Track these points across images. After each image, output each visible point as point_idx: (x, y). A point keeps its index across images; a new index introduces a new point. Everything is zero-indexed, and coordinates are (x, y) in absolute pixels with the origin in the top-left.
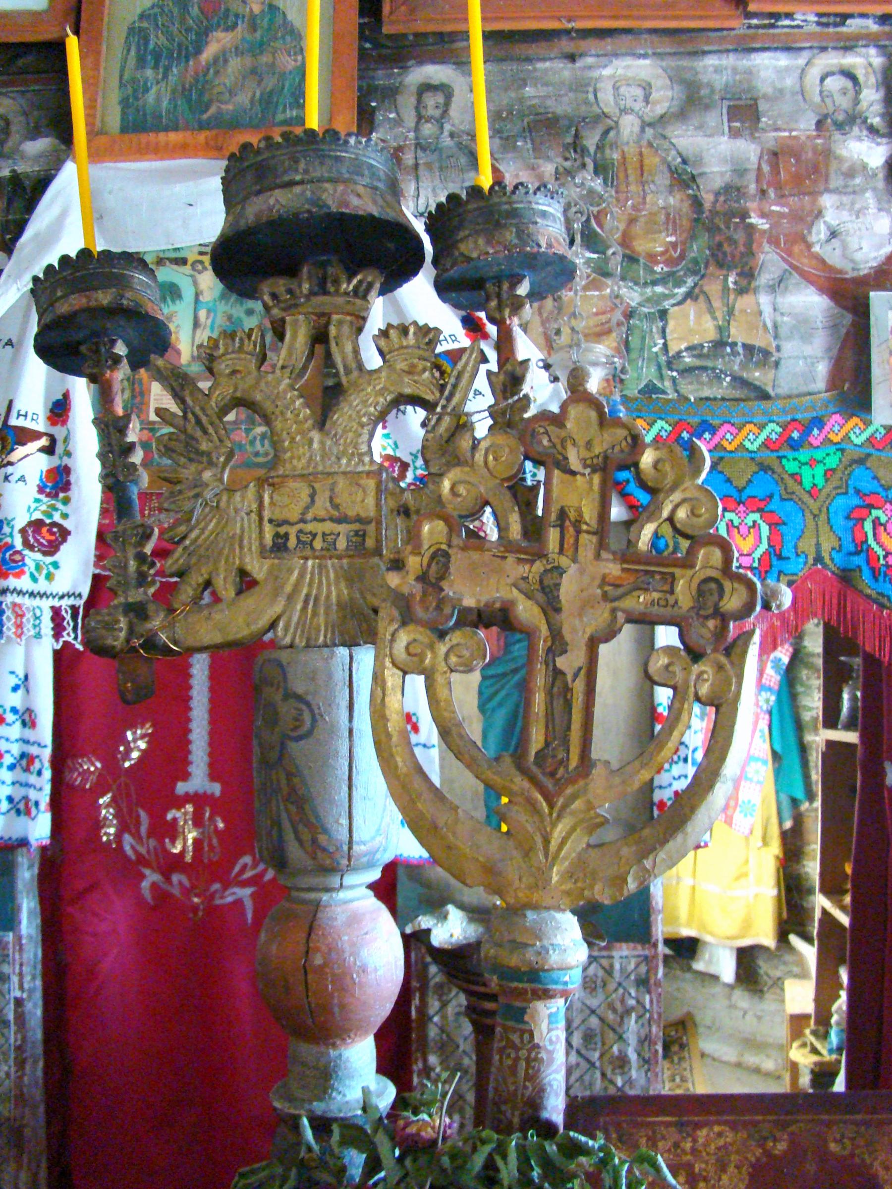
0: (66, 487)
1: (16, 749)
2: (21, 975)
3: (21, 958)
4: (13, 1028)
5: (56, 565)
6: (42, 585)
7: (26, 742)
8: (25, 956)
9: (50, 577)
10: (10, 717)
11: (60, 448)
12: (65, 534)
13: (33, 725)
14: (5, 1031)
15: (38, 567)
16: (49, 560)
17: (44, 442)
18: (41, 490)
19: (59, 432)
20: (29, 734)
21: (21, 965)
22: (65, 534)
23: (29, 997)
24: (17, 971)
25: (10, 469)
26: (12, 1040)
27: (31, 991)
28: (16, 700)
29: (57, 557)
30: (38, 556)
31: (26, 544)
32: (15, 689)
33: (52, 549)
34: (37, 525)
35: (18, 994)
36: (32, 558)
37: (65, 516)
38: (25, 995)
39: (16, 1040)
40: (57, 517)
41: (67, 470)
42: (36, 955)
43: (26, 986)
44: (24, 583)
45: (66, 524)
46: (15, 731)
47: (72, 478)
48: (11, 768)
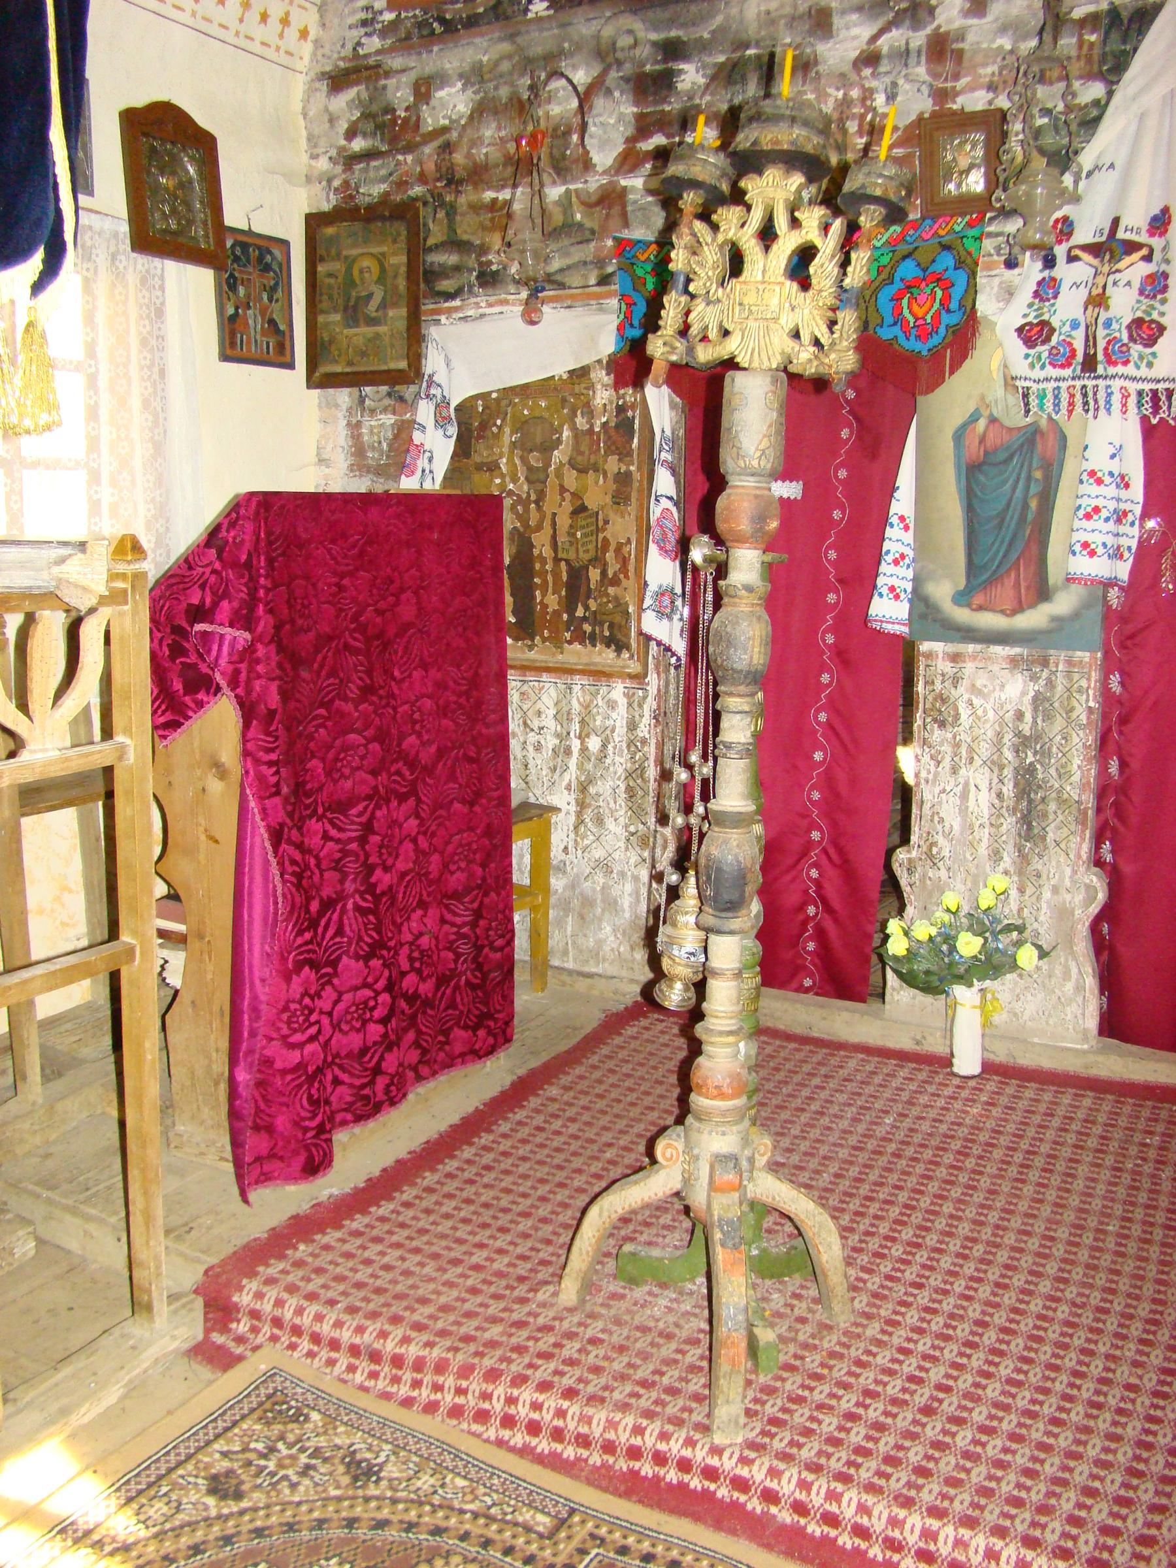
0: (1165, 289)
1: (1112, 505)
5: (1154, 355)
6: (1144, 372)
7: (1118, 500)
9: (1150, 365)
10: (1107, 479)
11: (1157, 256)
12: (1162, 329)
13: (1127, 486)
15: (1141, 358)
16: (1149, 350)
17: (1144, 252)
18: (1141, 293)
19: (1156, 242)
20: (1124, 494)
22: (1162, 329)
25: (1117, 276)
28: (1115, 466)
29: (1155, 349)
30: (1140, 348)
31: (1131, 338)
32: (1113, 457)
33: (1151, 341)
34: (1138, 323)
36: (1136, 349)
37: (1162, 314)
40: (1155, 316)
41: (1165, 276)
44: (1130, 370)
45: (1163, 321)
46: (1111, 491)
47: (1170, 282)
48: (1107, 520)
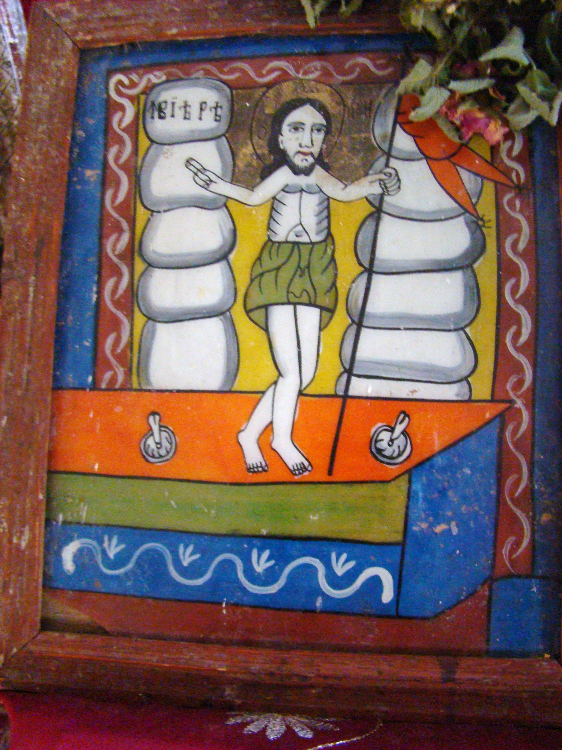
2: (10, 25)
3: (6, 11)
4: (14, 67)
8: (9, 9)
14: (9, 69)
21: (8, 16)
23: (20, 42)
24: (6, 22)
26: (16, 76)
27: (21, 38)
35: (12, 40)
38: (17, 41)
39: (19, 76)
42: (18, 11)
43: (16, 33)
